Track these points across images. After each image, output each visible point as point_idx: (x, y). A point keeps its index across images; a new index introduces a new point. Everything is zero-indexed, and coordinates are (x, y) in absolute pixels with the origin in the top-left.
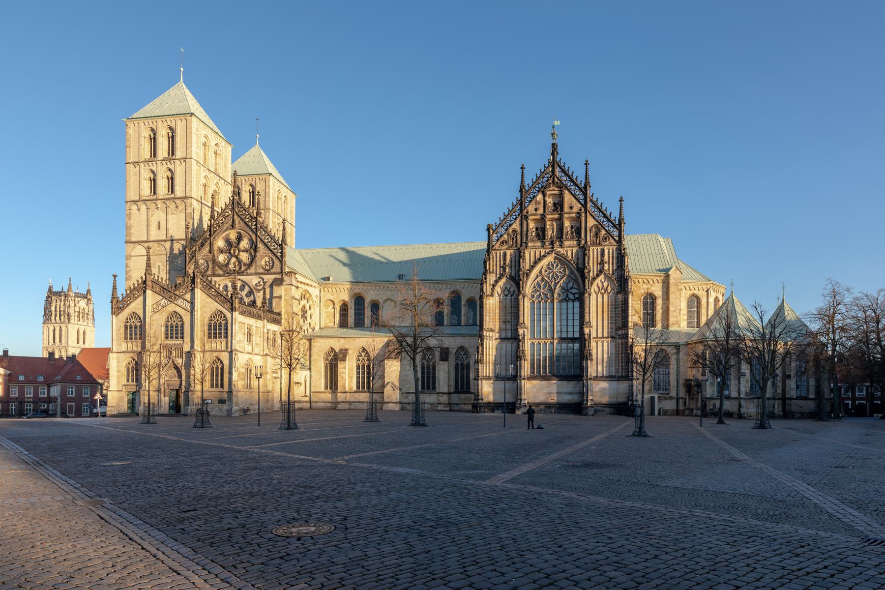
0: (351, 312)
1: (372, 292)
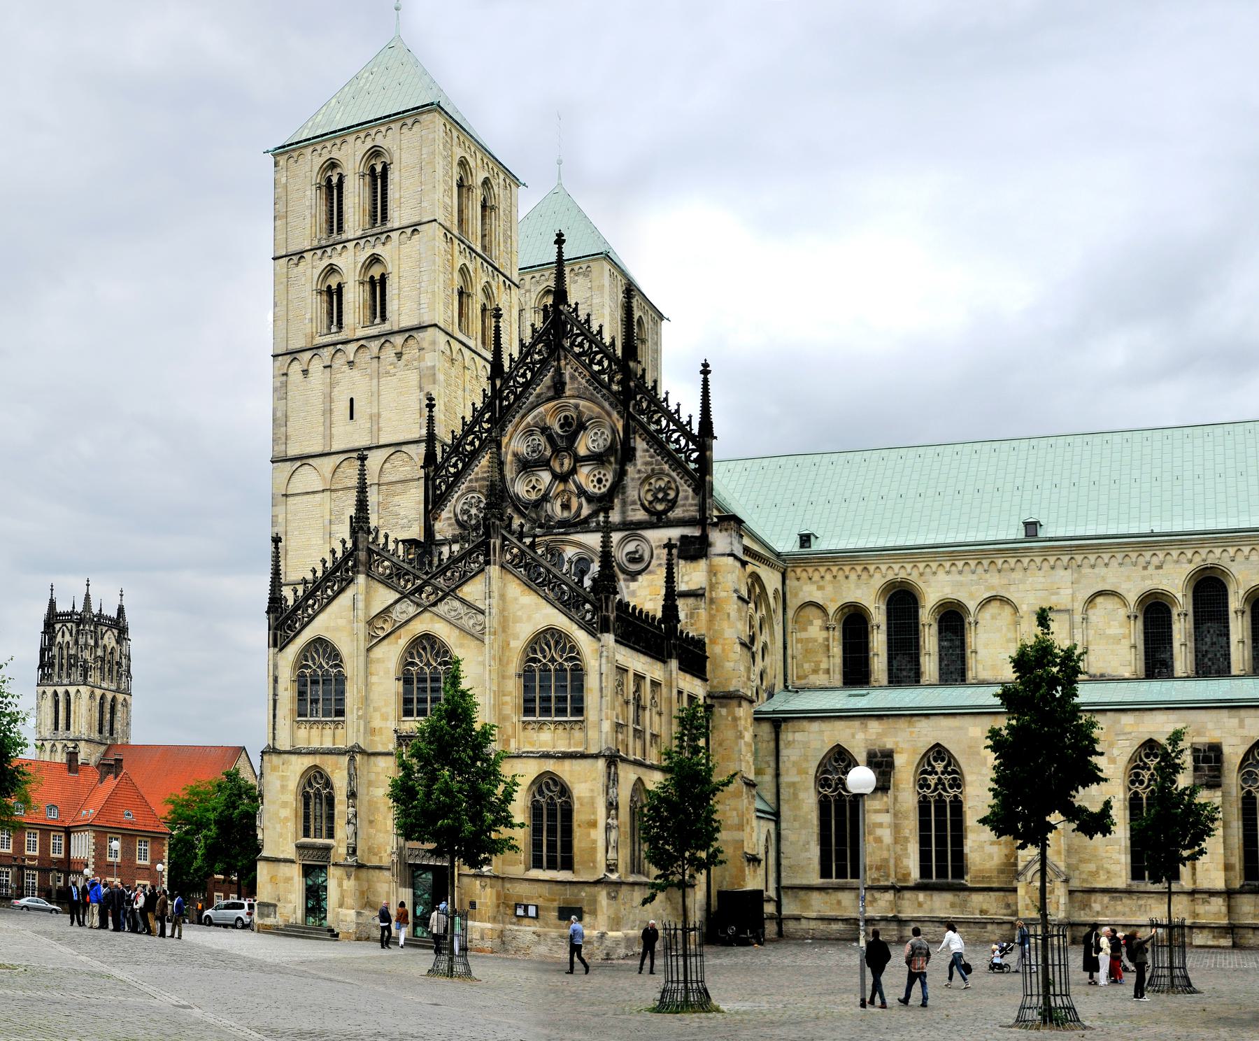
0: (879, 641)
1: (941, 575)
